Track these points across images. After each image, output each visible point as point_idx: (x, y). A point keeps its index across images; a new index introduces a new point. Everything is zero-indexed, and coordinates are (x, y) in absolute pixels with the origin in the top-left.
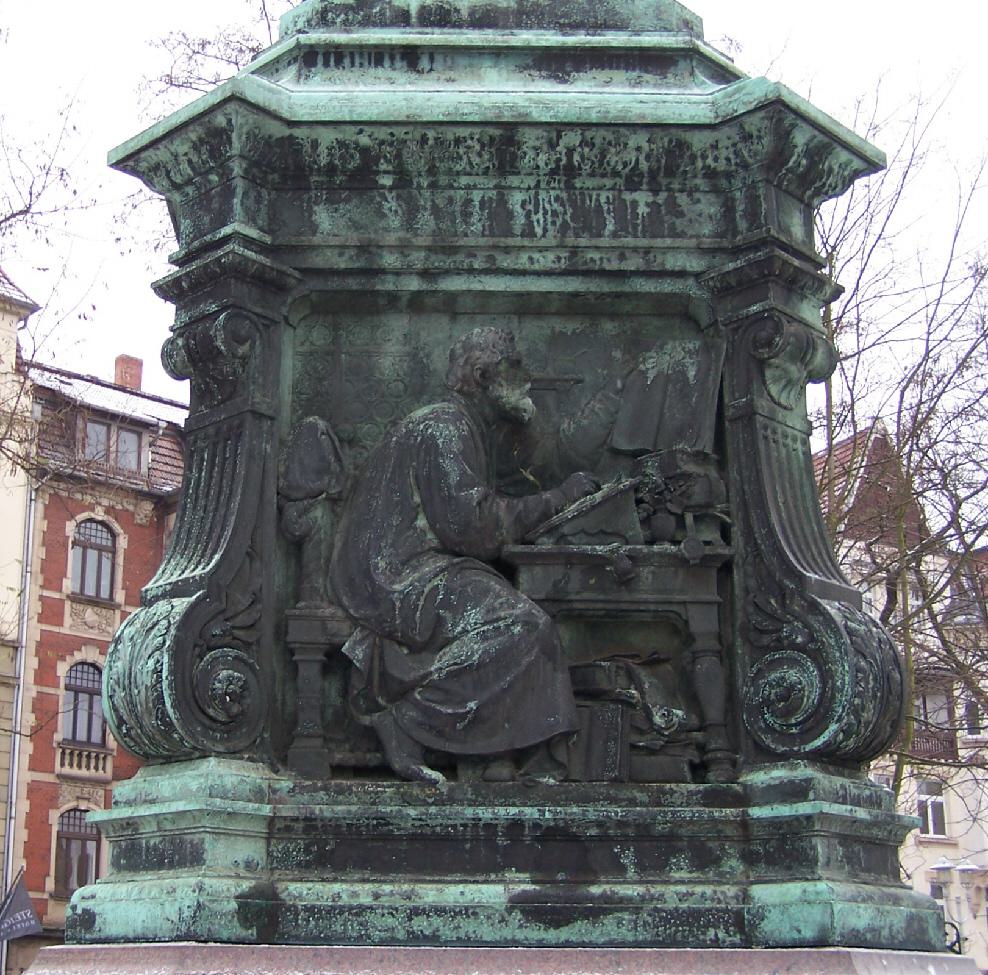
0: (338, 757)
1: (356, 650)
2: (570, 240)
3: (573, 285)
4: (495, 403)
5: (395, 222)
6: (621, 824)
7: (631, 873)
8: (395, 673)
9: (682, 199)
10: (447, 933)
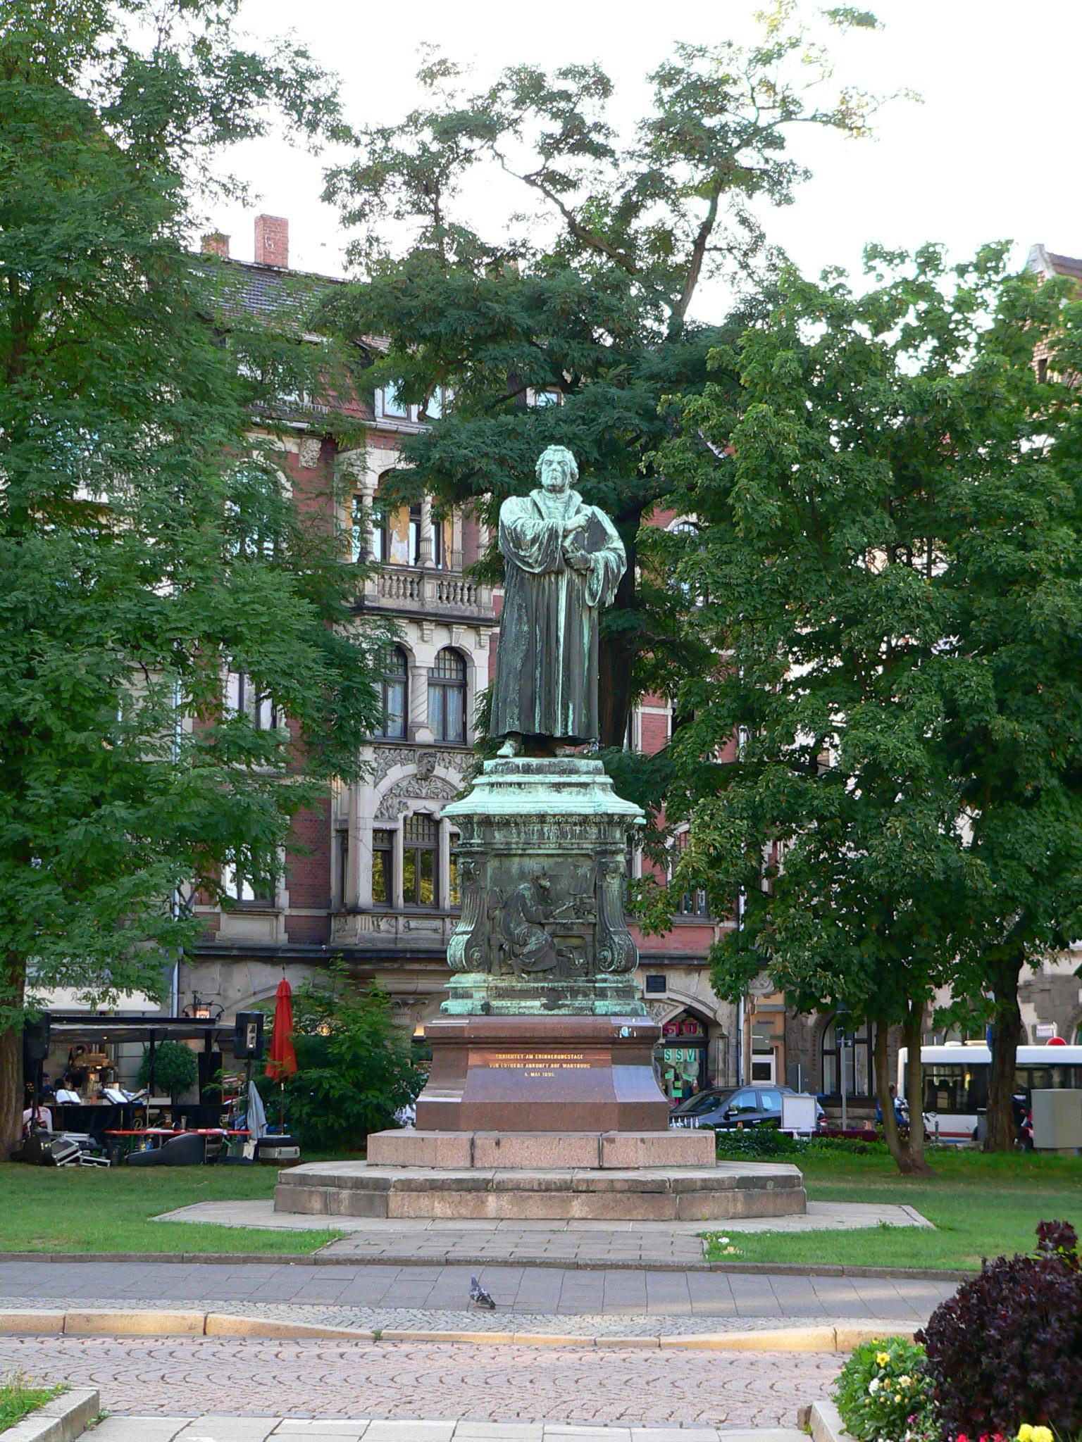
3: (560, 852)
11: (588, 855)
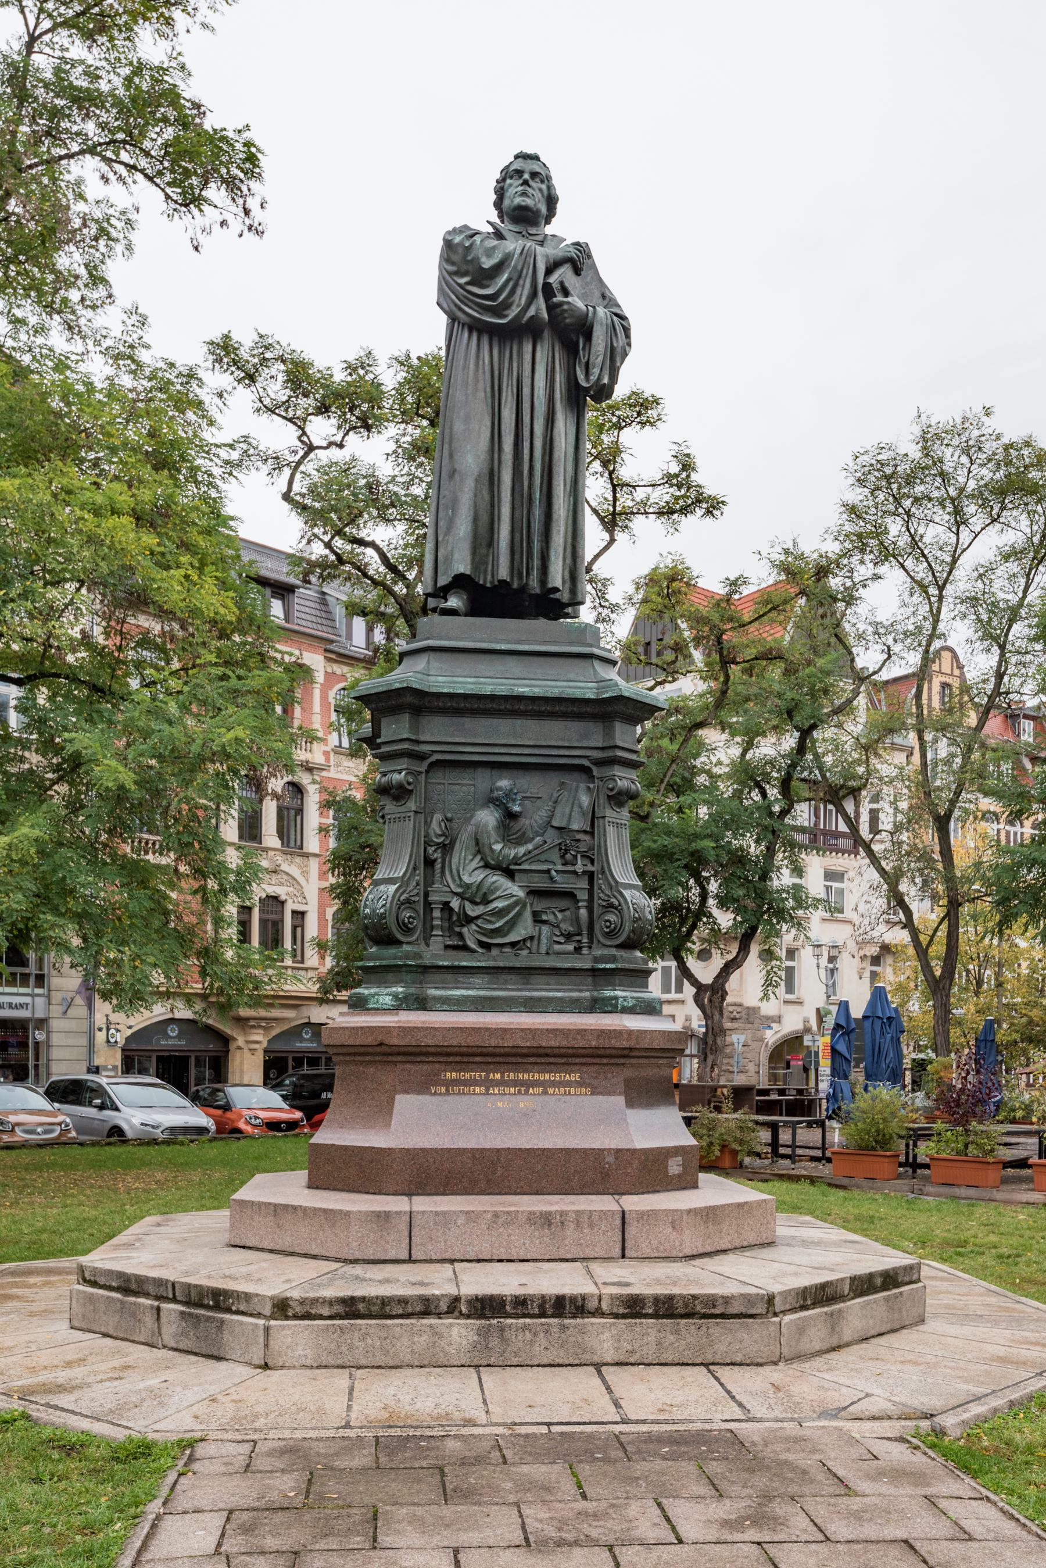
1: (455, 904)
8: (470, 913)
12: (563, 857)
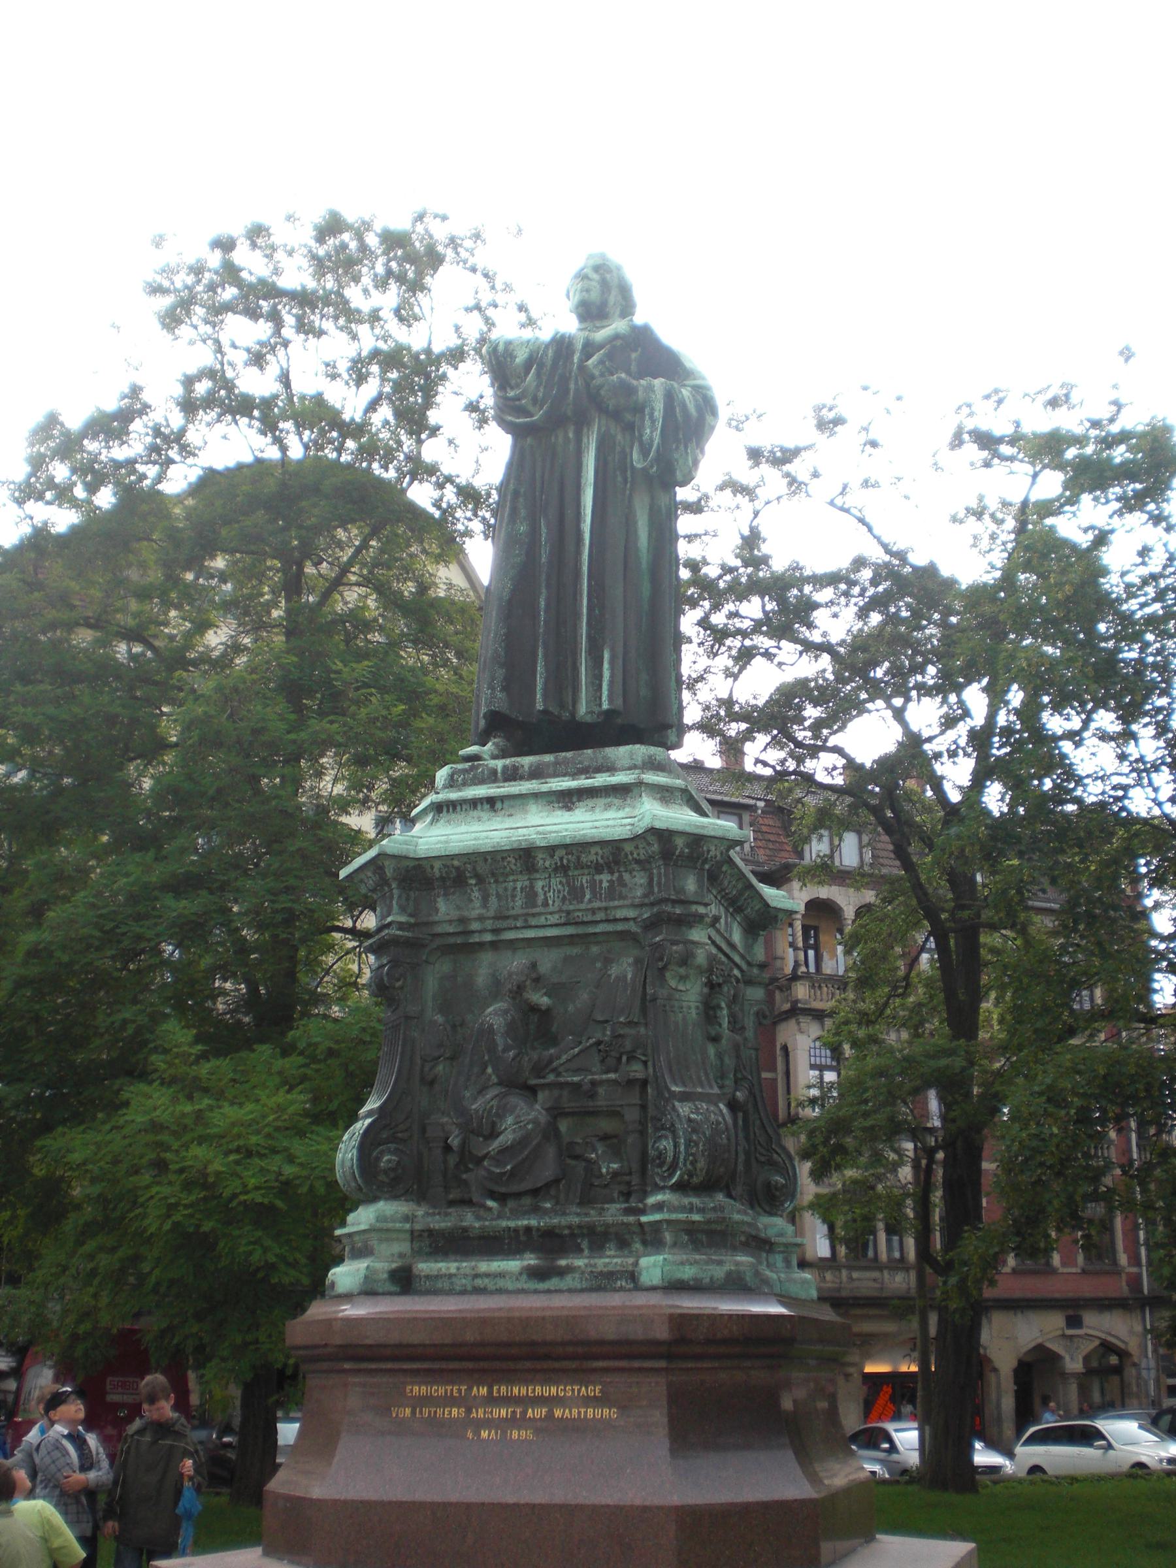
0: (451, 1196)
2: (565, 908)
4: (526, 1001)
5: (477, 904)
6: (580, 1227)
7: (586, 1252)
9: (626, 876)
10: (491, 1287)
11: (623, 935)
12: (602, 1061)
